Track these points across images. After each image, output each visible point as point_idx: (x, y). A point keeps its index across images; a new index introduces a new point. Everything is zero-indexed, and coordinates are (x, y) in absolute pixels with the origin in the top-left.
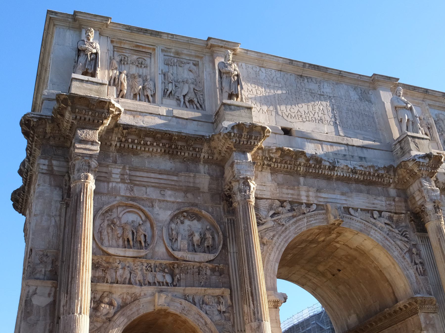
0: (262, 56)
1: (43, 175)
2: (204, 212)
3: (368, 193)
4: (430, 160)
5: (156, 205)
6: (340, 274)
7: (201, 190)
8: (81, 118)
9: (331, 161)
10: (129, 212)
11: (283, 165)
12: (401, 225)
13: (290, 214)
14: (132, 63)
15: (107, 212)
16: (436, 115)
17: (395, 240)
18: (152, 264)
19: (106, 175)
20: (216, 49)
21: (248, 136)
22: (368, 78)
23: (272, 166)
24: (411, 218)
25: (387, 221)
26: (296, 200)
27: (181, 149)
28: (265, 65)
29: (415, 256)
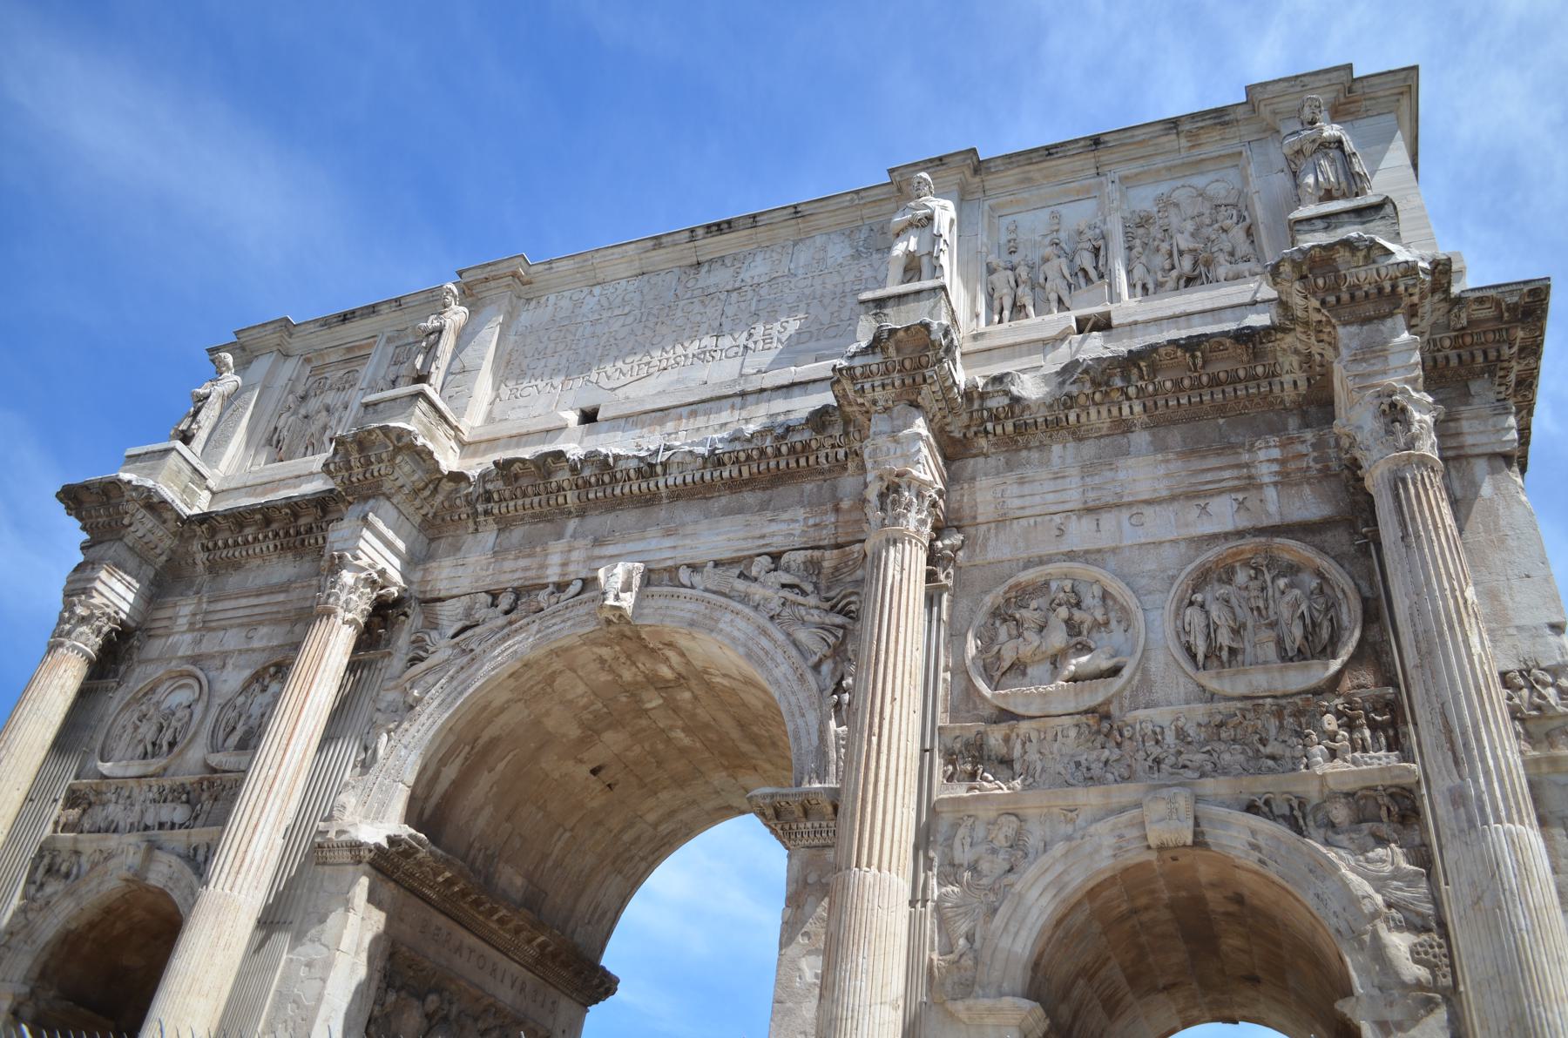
3: (763, 507)
4: (884, 350)
5: (230, 662)
9: (643, 454)
10: (181, 687)
12: (849, 579)
13: (502, 620)
14: (331, 388)
15: (145, 694)
17: (791, 630)
18: (167, 787)
22: (885, 189)
23: (496, 511)
27: (307, 533)
28: (601, 277)
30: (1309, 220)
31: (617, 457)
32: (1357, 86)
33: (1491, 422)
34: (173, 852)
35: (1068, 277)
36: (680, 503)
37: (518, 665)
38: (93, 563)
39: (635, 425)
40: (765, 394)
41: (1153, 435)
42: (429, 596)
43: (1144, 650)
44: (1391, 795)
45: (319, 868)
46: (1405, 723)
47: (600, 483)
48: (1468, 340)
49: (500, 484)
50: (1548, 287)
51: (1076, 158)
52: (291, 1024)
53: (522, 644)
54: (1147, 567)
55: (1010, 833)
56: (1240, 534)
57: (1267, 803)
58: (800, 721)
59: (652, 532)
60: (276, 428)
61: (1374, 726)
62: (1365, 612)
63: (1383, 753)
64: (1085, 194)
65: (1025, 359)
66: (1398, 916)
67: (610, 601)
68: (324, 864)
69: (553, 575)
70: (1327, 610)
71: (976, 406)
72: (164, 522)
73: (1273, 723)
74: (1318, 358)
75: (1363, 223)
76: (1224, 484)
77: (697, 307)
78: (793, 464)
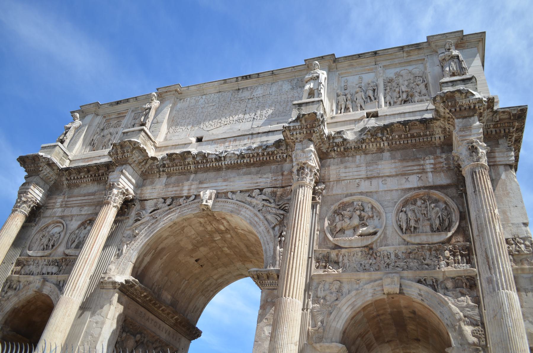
0: (201, 87)
3: (257, 173)
4: (300, 121)
5: (74, 218)
9: (217, 153)
12: (285, 198)
13: (167, 208)
14: (112, 127)
15: (45, 228)
17: (265, 215)
18: (51, 260)
20: (164, 95)
22: (303, 66)
23: (166, 171)
27: (102, 175)
28: (205, 92)
30: (447, 82)
31: (208, 154)
32: (465, 38)
33: (505, 153)
34: (52, 282)
35: (364, 98)
36: (229, 170)
37: (172, 223)
38: (29, 183)
39: (215, 143)
40: (260, 134)
41: (391, 153)
42: (142, 199)
43: (385, 227)
44: (467, 279)
45: (102, 290)
46: (473, 255)
48: (499, 125)
49: (168, 162)
50: (527, 108)
51: (369, 58)
52: (89, 343)
53: (174, 216)
54: (387, 198)
55: (337, 287)
56: (419, 188)
57: (425, 280)
58: (267, 246)
59: (219, 180)
60: (93, 140)
61: (462, 255)
62: (461, 216)
63: (465, 265)
64: (371, 71)
65: (348, 126)
66: (468, 320)
67: (204, 203)
68: (103, 288)
69: (185, 193)
70: (448, 215)
71: (331, 141)
72: (53, 170)
73: (428, 253)
74: (448, 129)
75: (465, 84)
76: (414, 171)
77: (238, 104)
78: (268, 159)
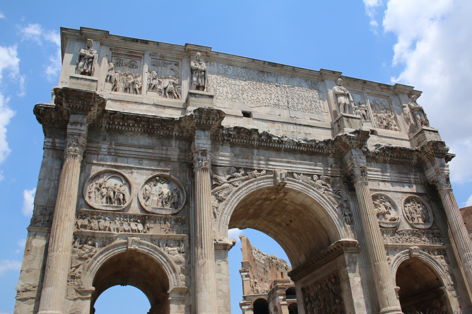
1: (48, 150)
2: (172, 177)
4: (359, 135)
6: (292, 225)
7: (172, 160)
8: (73, 106)
9: (280, 137)
10: (113, 177)
11: (240, 140)
12: (336, 186)
13: (243, 178)
16: (373, 101)
19: (96, 149)
21: (207, 118)
22: (317, 73)
23: (231, 140)
24: (344, 180)
25: (324, 183)
26: (249, 167)
27: (157, 129)
29: (345, 209)
47: (266, 142)
49: (235, 133)
64: (358, 93)
78: (318, 151)
